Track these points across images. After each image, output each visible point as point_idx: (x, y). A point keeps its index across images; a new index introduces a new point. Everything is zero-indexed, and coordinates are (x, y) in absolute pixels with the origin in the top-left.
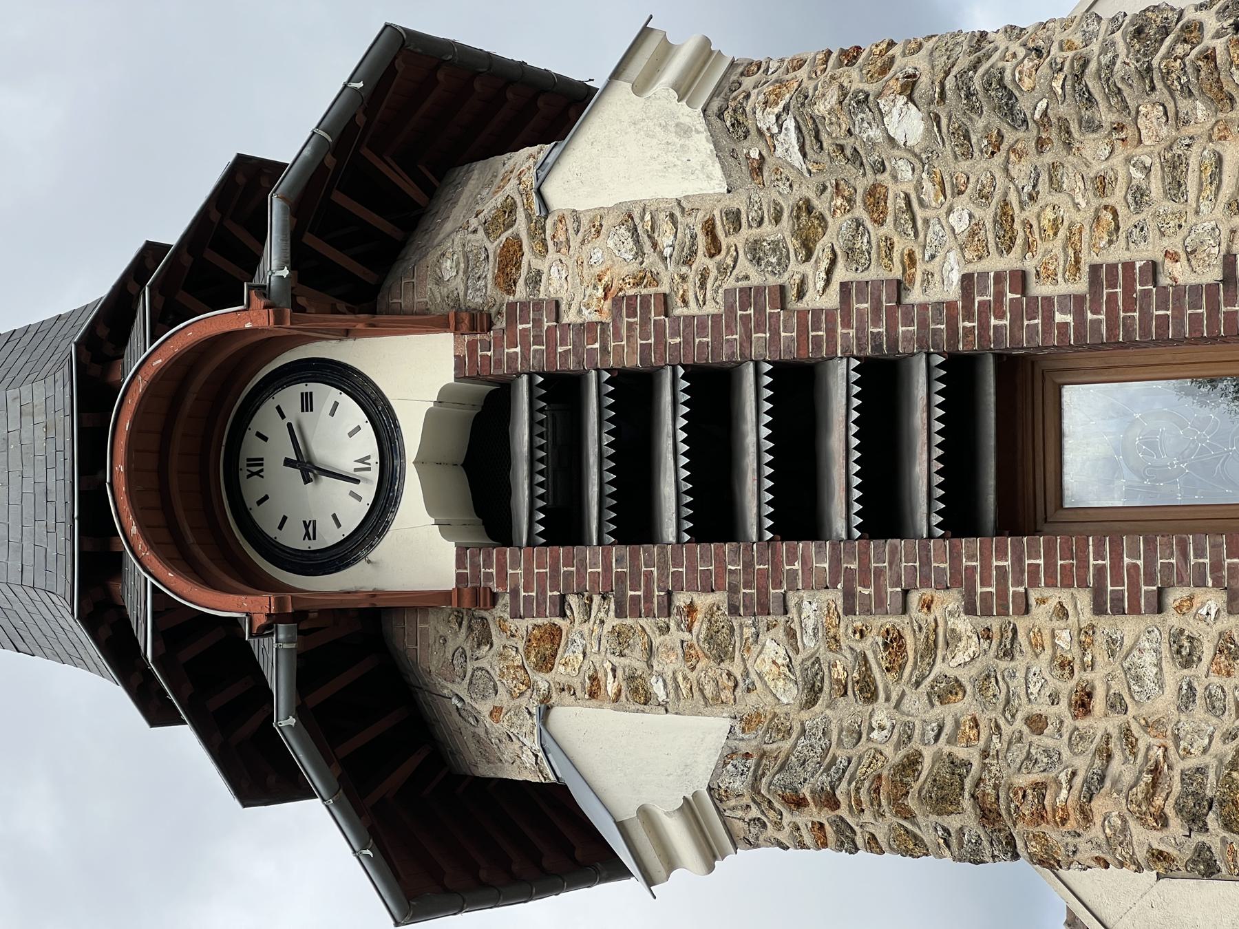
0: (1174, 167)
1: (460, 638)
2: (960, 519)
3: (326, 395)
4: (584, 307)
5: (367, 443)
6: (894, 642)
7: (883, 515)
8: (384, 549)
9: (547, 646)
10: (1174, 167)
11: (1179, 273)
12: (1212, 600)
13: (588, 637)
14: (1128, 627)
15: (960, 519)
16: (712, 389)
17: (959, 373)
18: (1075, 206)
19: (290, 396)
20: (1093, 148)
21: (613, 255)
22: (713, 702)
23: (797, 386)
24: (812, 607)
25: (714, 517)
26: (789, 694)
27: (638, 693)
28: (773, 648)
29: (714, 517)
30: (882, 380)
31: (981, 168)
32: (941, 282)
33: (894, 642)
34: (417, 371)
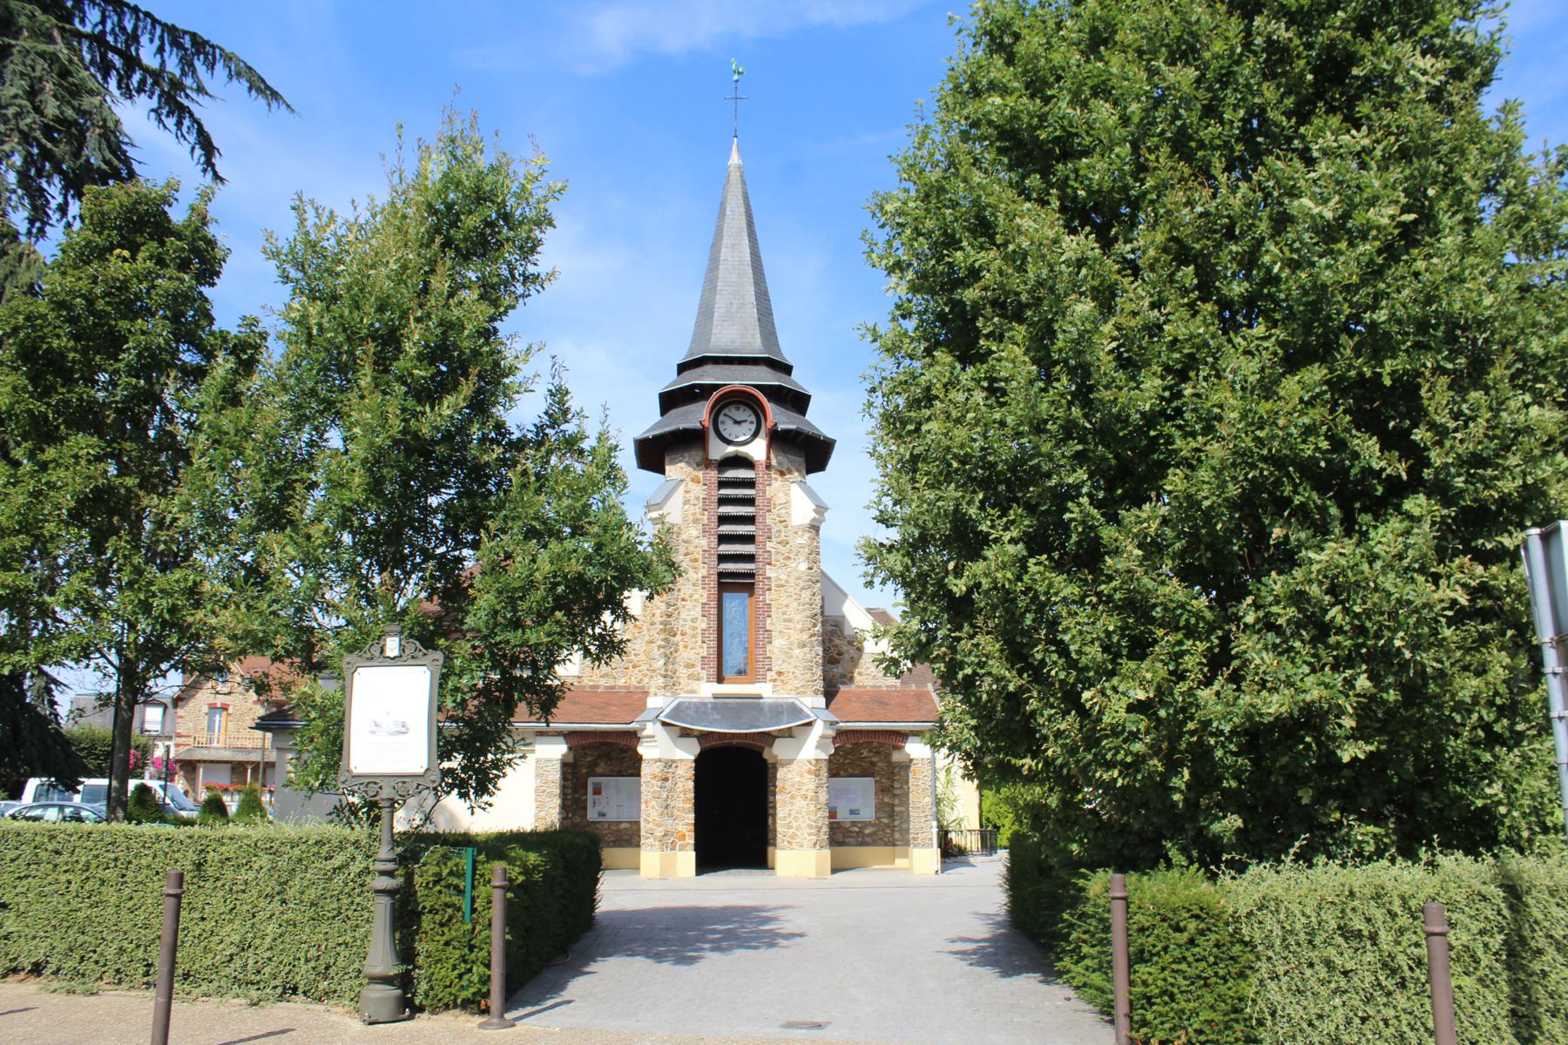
0: (790, 620)
1: (698, 459)
2: (721, 575)
3: (753, 427)
4: (770, 491)
5: (742, 439)
6: (696, 560)
7: (723, 558)
8: (718, 441)
9: (696, 480)
10: (790, 620)
11: (769, 621)
12: (704, 626)
13: (698, 491)
14: (699, 609)
15: (721, 575)
16: (750, 520)
17: (751, 575)
18: (784, 600)
19: (753, 418)
20: (795, 605)
21: (780, 498)
22: (685, 520)
23: (749, 539)
24: (704, 542)
25: (723, 520)
26: (684, 537)
27: (686, 502)
28: (695, 533)
29: (723, 520)
30: (750, 558)
31: (792, 580)
32: (770, 572)
33: (696, 560)
34: (757, 450)
